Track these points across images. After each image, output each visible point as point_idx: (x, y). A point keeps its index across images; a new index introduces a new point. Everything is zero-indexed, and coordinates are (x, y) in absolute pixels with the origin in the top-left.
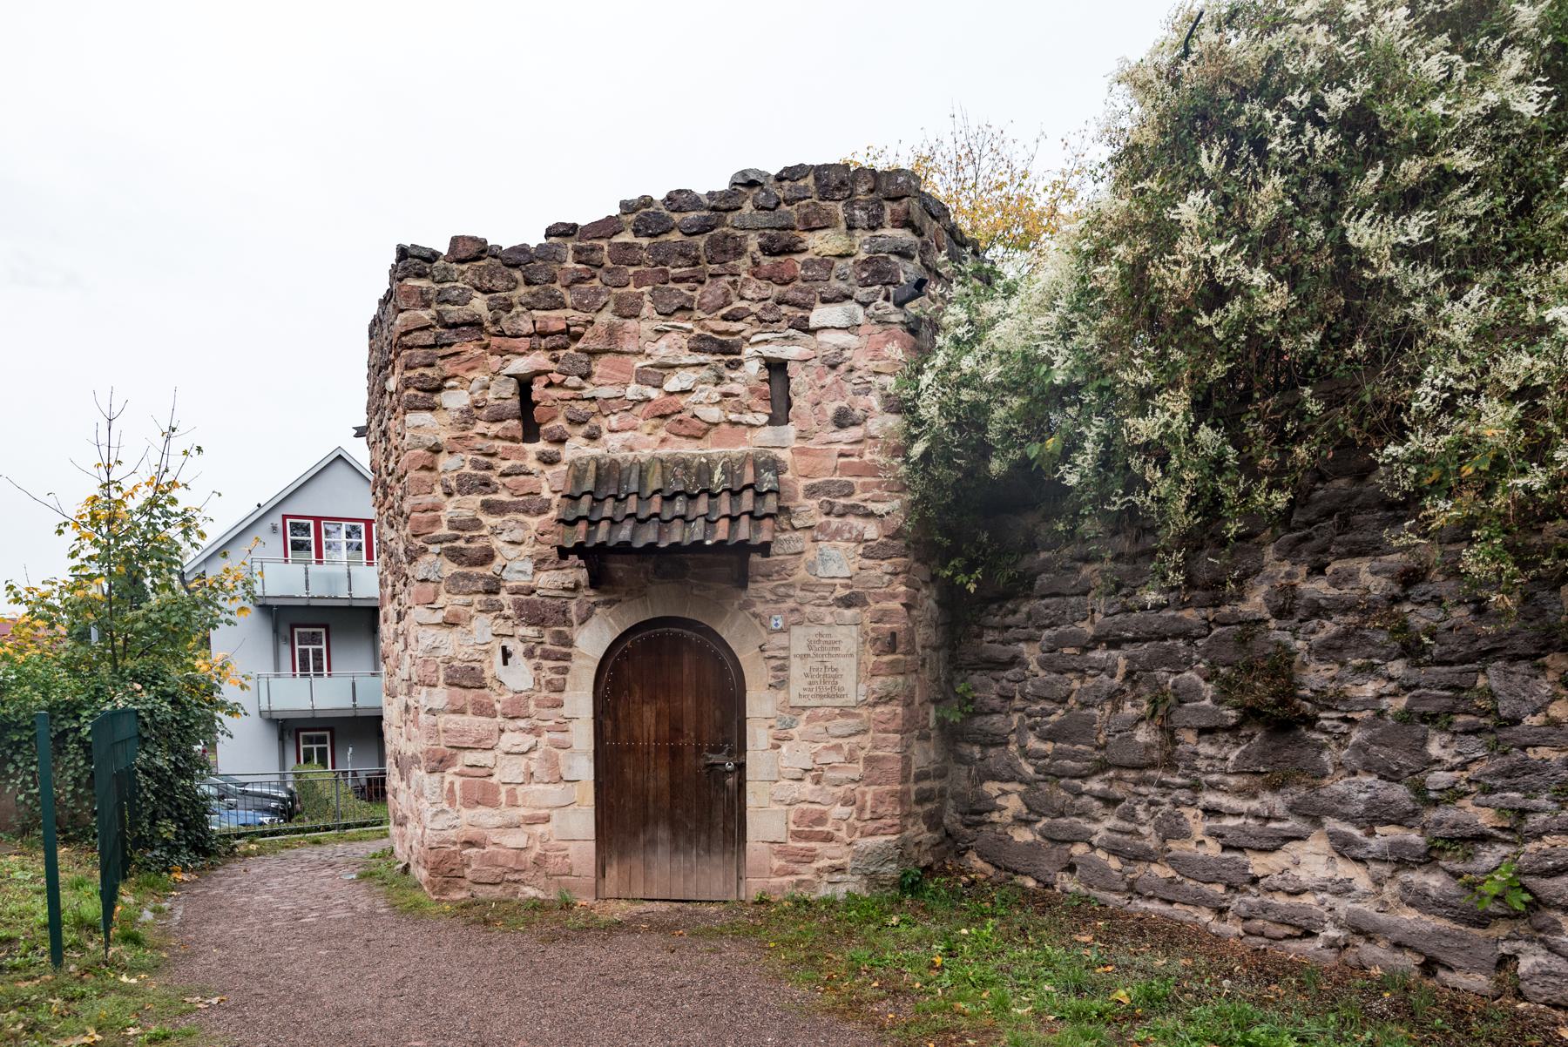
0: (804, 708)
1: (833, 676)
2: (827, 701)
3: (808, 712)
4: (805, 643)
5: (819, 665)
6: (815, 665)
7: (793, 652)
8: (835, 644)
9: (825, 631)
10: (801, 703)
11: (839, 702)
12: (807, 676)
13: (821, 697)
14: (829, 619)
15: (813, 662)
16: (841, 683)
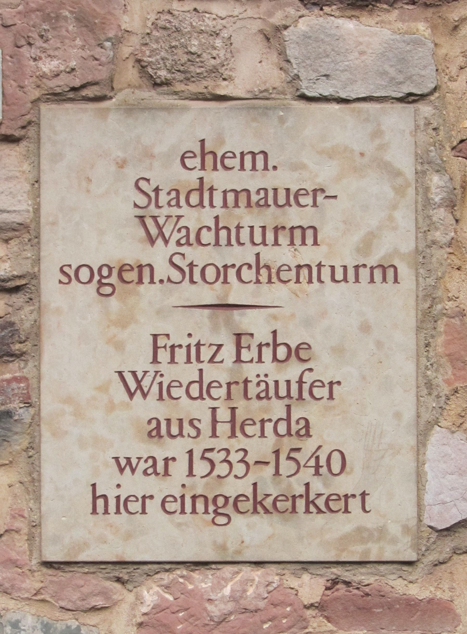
0: (125, 571)
1: (279, 396)
2: (252, 533)
3: (151, 594)
4: (124, 202)
5: (202, 327)
6: (179, 329)
7: (56, 252)
8: (287, 214)
9: (234, 132)
10: (106, 540)
11: (315, 537)
12: (134, 386)
13: (219, 508)
14: (251, 69)
15: (160, 310)
16: (329, 431)
